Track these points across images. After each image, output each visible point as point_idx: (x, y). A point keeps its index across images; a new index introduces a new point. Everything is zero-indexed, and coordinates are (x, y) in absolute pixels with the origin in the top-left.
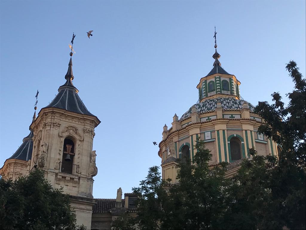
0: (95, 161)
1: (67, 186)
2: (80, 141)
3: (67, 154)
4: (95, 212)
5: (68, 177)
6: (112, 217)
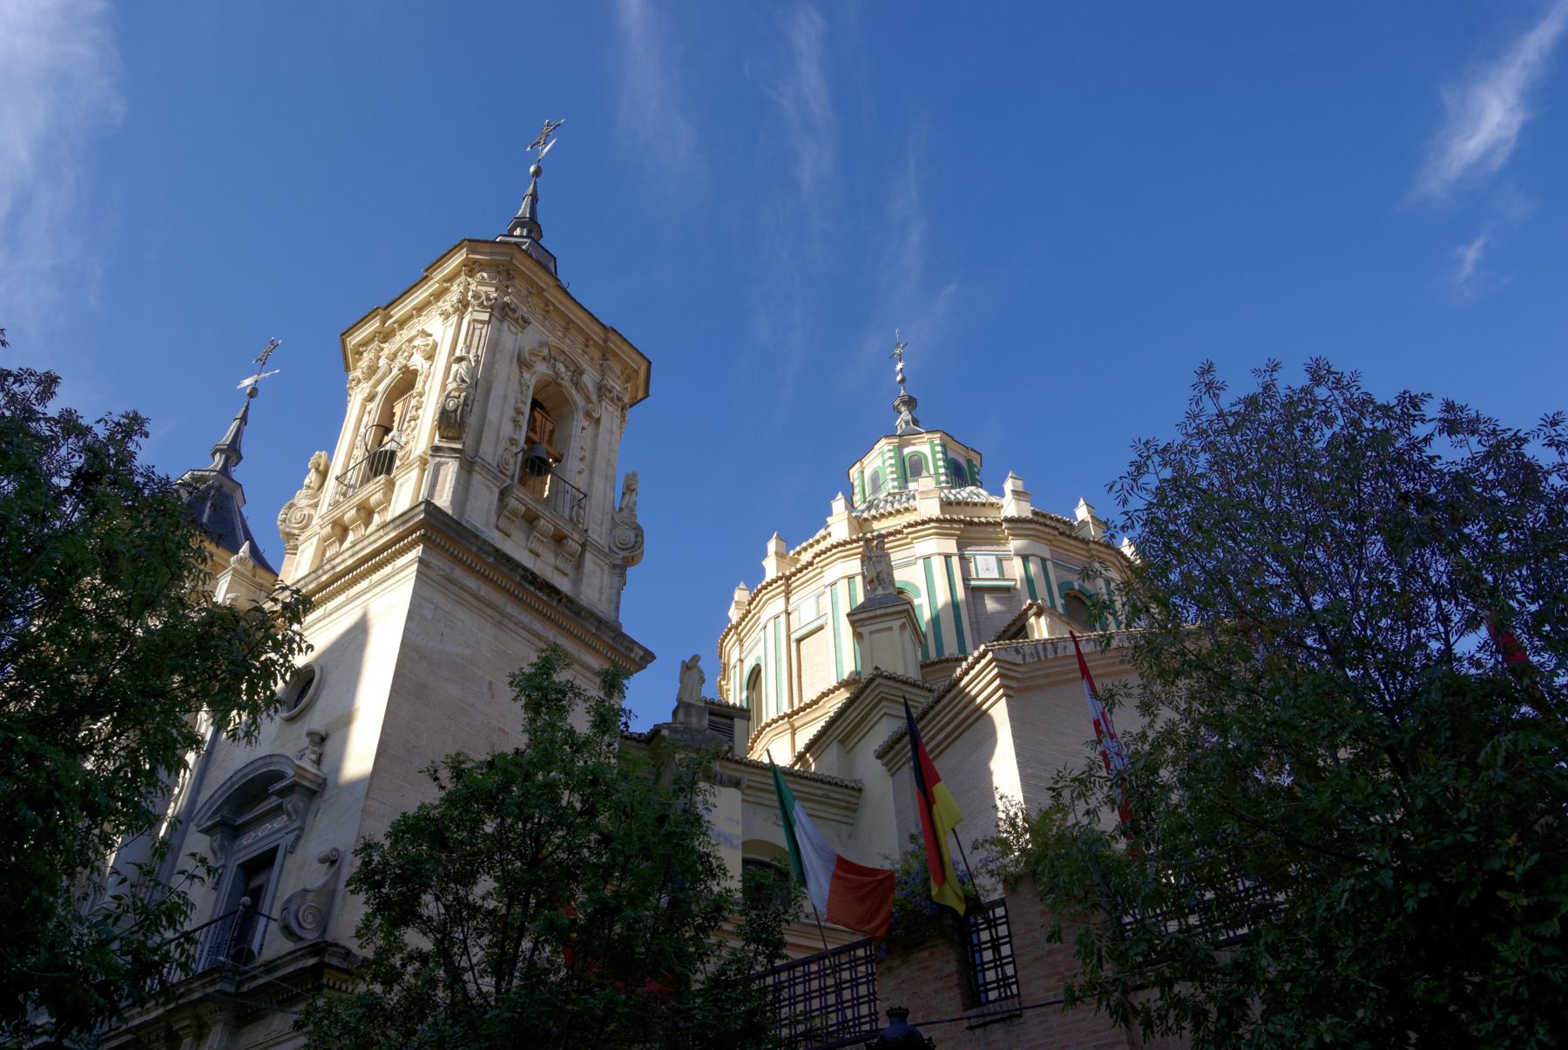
1: (533, 556)
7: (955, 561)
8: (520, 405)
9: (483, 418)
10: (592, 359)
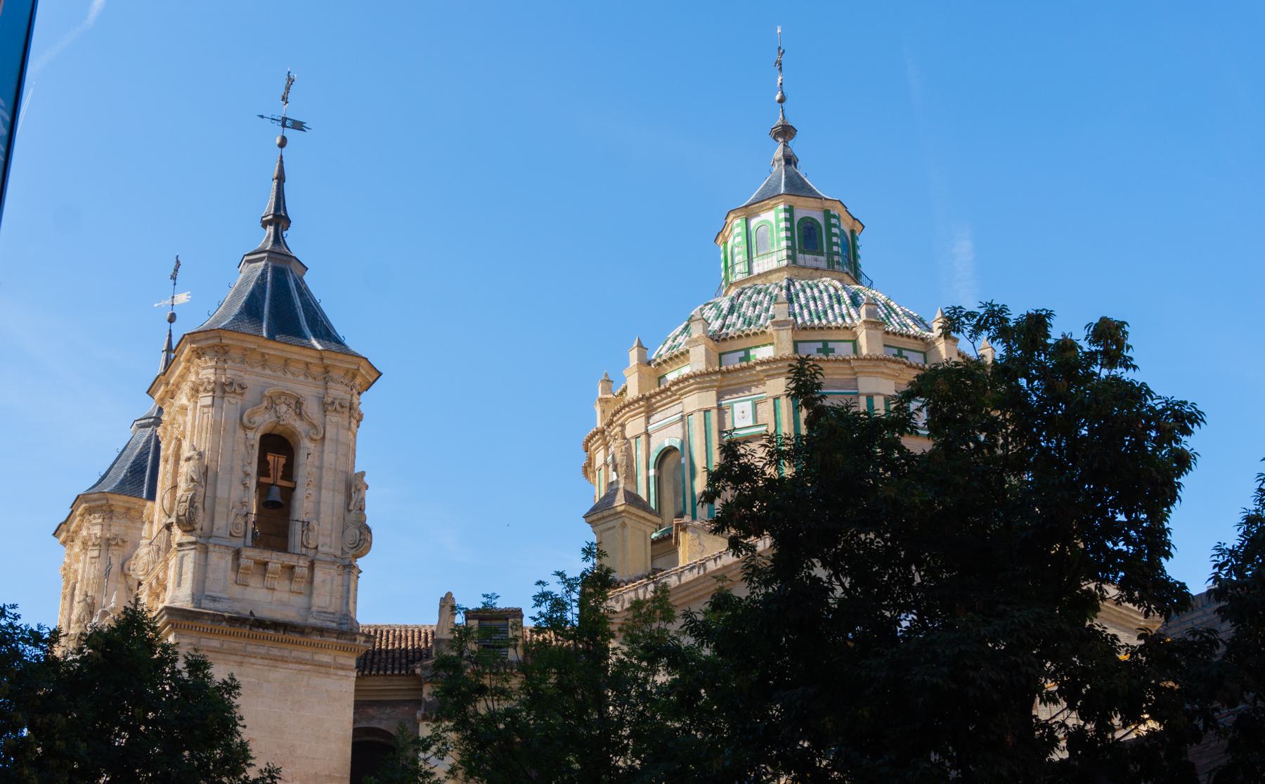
0: (362, 509)
1: (270, 592)
2: (312, 439)
3: (273, 485)
4: (366, 673)
5: (276, 560)
6: (421, 690)
7: (714, 415)
8: (248, 469)
9: (215, 497)
10: (315, 379)
